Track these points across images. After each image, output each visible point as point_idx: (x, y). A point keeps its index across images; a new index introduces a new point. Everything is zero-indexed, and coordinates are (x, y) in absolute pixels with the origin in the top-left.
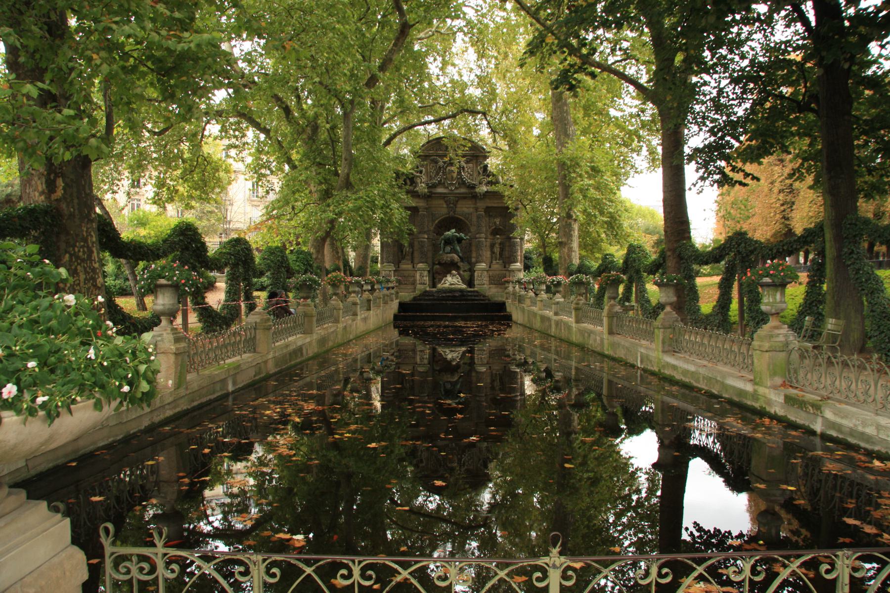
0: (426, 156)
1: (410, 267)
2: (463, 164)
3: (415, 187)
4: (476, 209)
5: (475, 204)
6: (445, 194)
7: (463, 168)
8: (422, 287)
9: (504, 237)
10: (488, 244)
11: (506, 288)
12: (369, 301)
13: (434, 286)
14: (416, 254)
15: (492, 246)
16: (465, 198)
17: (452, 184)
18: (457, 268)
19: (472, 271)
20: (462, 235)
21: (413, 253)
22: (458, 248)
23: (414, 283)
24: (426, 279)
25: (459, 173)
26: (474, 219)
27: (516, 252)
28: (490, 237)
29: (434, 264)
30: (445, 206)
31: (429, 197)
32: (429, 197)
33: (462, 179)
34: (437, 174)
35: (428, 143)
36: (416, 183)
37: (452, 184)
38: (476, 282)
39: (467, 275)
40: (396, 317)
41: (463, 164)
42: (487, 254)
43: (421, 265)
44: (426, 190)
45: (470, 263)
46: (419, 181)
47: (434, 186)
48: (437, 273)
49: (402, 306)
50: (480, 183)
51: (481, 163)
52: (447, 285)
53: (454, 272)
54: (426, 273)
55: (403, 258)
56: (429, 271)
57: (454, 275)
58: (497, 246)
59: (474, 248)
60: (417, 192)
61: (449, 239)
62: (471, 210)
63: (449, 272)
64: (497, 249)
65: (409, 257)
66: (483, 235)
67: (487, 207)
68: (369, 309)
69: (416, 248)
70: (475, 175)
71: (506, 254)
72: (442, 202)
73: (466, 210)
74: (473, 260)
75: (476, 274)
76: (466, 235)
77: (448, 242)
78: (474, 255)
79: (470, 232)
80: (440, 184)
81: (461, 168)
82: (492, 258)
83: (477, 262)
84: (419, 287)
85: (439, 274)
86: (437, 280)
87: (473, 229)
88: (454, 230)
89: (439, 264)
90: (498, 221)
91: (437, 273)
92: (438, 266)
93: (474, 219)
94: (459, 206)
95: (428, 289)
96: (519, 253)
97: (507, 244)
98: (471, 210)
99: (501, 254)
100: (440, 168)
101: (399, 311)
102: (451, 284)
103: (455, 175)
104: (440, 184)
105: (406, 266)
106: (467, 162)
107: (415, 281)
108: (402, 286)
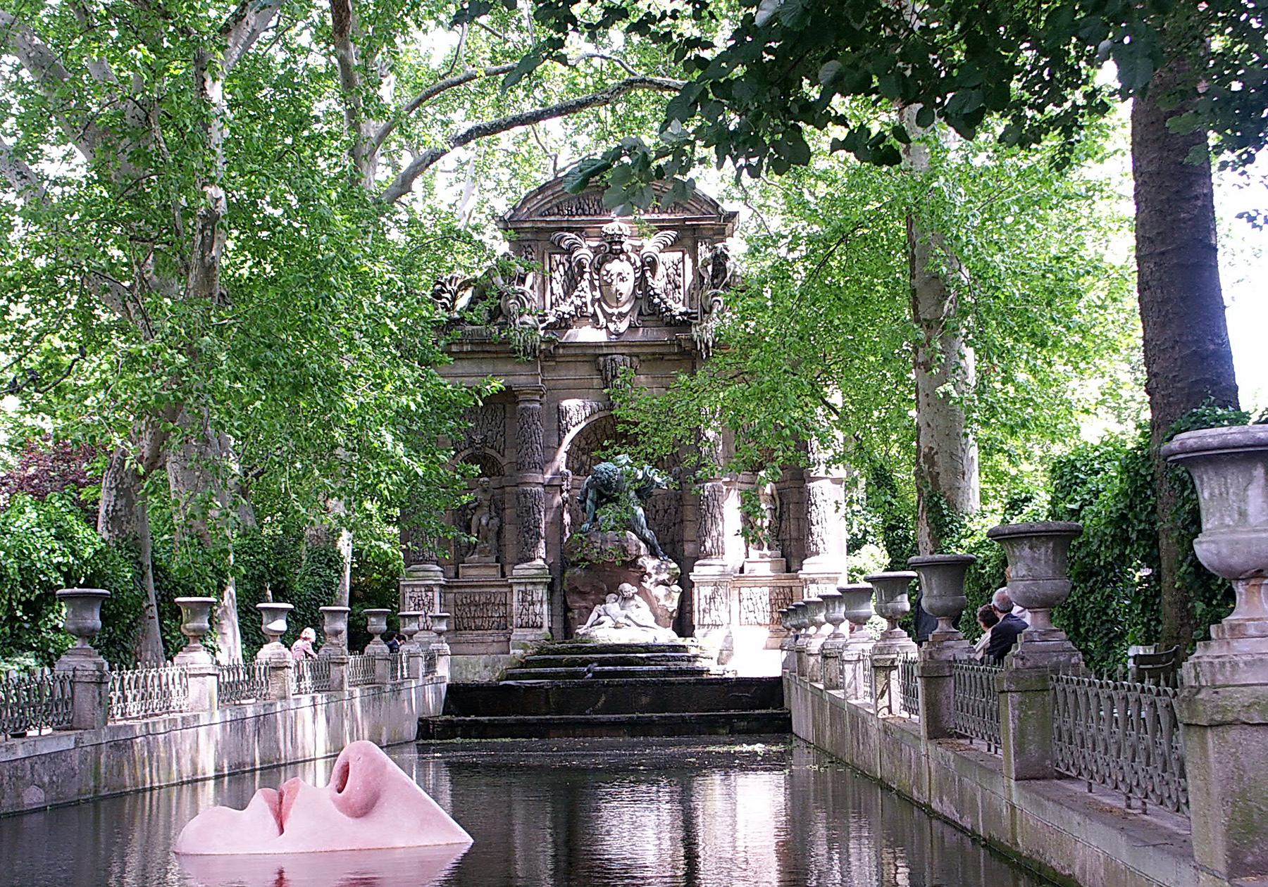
1: (494, 572)
3: (503, 326)
6: (597, 345)
8: (530, 635)
13: (568, 632)
21: (499, 533)
23: (504, 625)
25: (641, 282)
30: (597, 382)
31: (549, 356)
32: (549, 356)
40: (426, 728)
48: (575, 590)
53: (627, 588)
54: (541, 593)
56: (550, 587)
59: (689, 513)
60: (507, 341)
63: (614, 588)
71: (791, 527)
74: (689, 548)
77: (605, 492)
78: (689, 533)
84: (517, 634)
85: (583, 595)
91: (575, 590)
103: (626, 288)
105: (478, 571)
107: (507, 617)
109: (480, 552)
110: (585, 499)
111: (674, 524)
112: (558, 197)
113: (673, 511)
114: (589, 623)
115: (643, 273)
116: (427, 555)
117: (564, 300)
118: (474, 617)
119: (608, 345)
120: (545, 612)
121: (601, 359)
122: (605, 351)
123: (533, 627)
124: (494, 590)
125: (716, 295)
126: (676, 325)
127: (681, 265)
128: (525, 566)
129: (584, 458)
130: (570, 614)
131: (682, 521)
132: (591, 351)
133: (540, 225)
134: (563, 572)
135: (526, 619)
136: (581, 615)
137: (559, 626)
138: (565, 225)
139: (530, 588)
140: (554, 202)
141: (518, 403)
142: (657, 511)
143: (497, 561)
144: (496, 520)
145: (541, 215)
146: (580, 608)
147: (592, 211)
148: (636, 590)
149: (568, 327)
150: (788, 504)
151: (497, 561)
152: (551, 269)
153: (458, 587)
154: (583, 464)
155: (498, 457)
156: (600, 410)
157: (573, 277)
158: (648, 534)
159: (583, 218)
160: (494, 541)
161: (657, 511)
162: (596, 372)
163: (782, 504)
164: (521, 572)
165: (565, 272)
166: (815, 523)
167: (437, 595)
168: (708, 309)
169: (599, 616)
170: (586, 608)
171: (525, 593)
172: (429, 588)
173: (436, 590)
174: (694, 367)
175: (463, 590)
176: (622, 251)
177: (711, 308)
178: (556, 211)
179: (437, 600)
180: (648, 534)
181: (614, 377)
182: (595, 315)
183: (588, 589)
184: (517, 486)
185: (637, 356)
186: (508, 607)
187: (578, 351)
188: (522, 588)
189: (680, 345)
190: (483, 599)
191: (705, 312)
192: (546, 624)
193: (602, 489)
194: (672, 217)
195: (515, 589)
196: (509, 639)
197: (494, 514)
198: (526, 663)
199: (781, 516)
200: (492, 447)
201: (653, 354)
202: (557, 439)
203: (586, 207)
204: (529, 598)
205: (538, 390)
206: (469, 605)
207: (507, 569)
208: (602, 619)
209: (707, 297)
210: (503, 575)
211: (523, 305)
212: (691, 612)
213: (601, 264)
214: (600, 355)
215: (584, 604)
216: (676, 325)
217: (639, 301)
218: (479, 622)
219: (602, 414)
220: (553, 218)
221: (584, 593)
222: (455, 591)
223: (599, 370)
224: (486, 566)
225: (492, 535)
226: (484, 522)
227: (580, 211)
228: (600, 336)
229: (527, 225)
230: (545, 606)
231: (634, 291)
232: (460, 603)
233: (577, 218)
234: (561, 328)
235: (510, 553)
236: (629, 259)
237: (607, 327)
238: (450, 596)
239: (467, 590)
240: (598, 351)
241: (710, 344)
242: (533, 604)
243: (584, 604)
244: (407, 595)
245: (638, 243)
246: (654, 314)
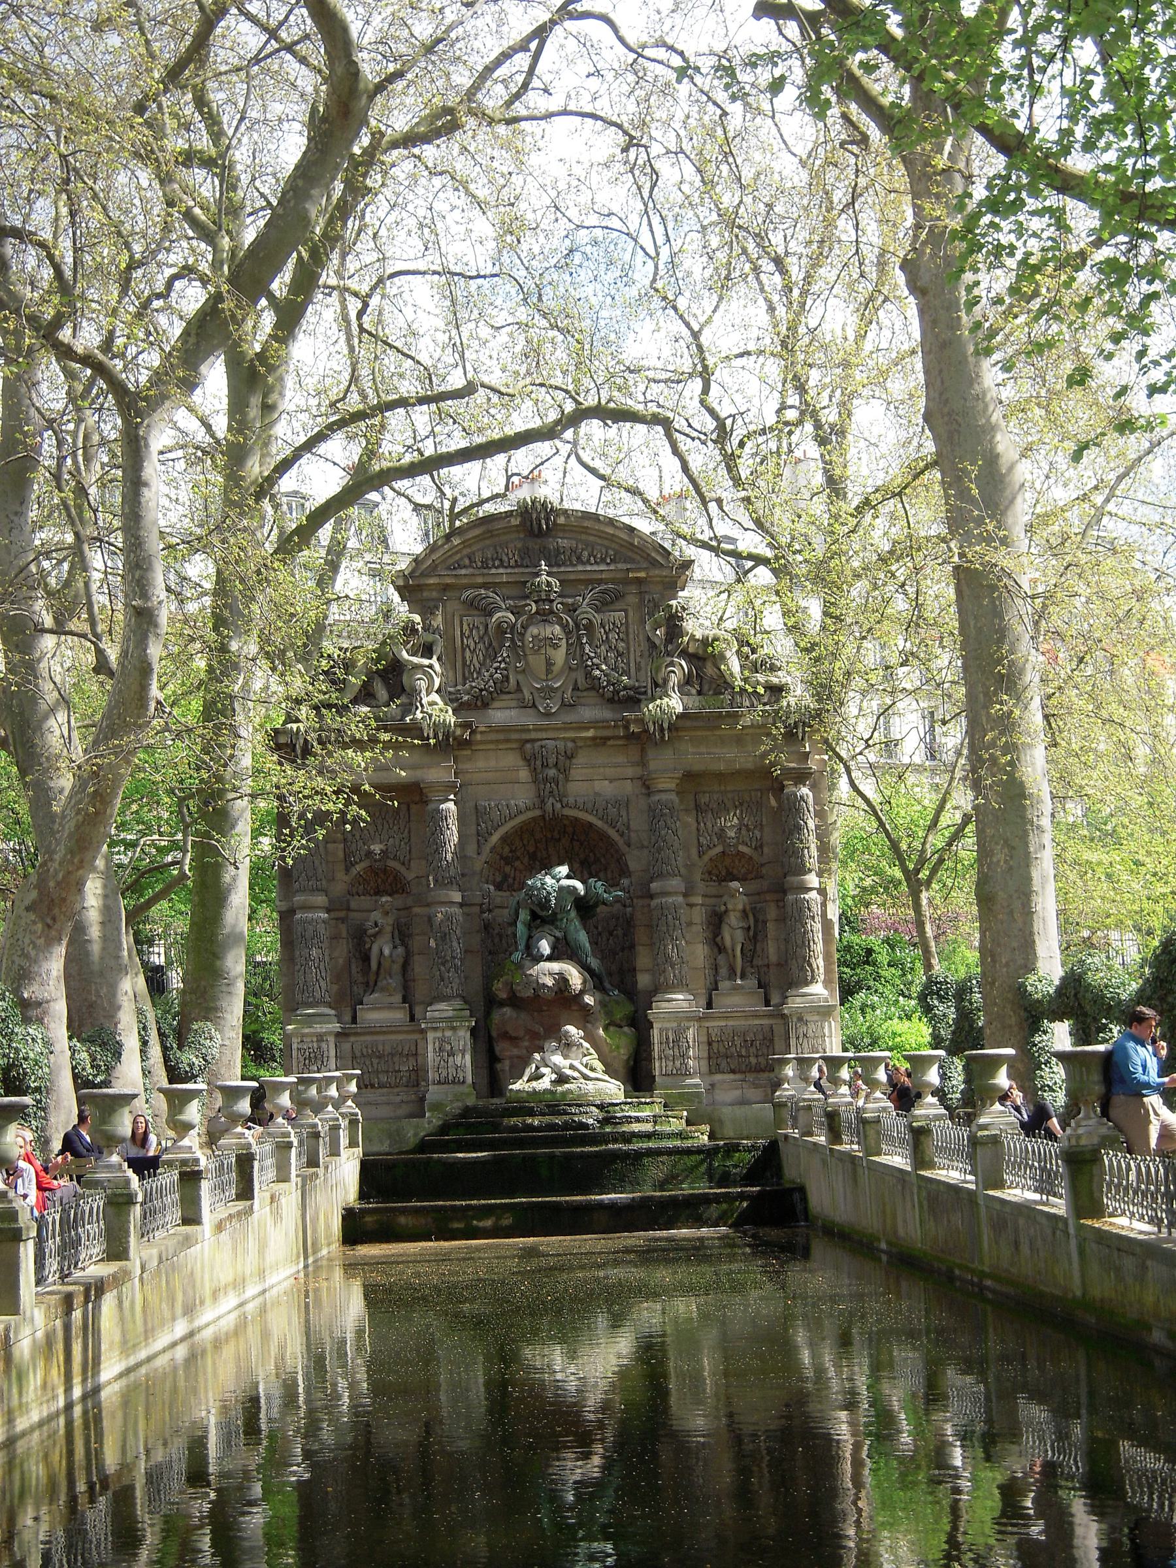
0: (446, 588)
1: (399, 1016)
2: (586, 611)
3: (409, 708)
4: (646, 785)
5: (643, 763)
6: (525, 729)
7: (590, 627)
9: (754, 886)
10: (698, 916)
11: (777, 1085)
12: (245, 1162)
14: (419, 967)
15: (716, 921)
16: (599, 742)
17: (548, 692)
18: (584, 1017)
19: (639, 1025)
20: (599, 887)
21: (406, 965)
22: (583, 938)
24: (466, 1060)
25: (575, 649)
26: (638, 822)
27: (804, 942)
28: (701, 887)
29: (491, 1002)
30: (524, 774)
32: (463, 744)
33: (588, 675)
34: (492, 653)
35: (448, 537)
36: (414, 693)
37: (548, 692)
38: (657, 1067)
39: (622, 1045)
40: (349, 1216)
41: (586, 611)
42: (698, 953)
43: (443, 1009)
44: (450, 718)
45: (630, 992)
46: (423, 684)
47: (480, 702)
48: (505, 1036)
49: (369, 1171)
50: (659, 687)
51: (656, 606)
52: (544, 1084)
53: (571, 1029)
54: (463, 1038)
55: (370, 986)
56: (474, 1032)
57: (567, 1046)
58: (733, 919)
59: (641, 935)
61: (544, 904)
62: (628, 787)
63: (553, 1031)
64: (733, 935)
65: (394, 982)
66: (675, 883)
67: (690, 777)
68: (246, 1192)
69: (416, 943)
70: (637, 648)
71: (772, 950)
72: (511, 759)
73: (606, 789)
74: (643, 980)
75: (655, 1033)
76: (612, 884)
78: (643, 959)
79: (624, 871)
80: (501, 689)
81: (578, 632)
82: (716, 968)
83: (658, 989)
84: (434, 1093)
85: (514, 1040)
86: (506, 1065)
87: (635, 861)
88: (563, 870)
89: (514, 1001)
90: (730, 822)
91: (505, 1036)
92: (507, 1011)
93: (638, 822)
94: (575, 773)
95: (471, 1101)
96: (819, 947)
97: (772, 913)
98: (628, 787)
99: (751, 953)
100: (500, 630)
101: (363, 1195)
102: (562, 1079)
103: (559, 656)
104: (501, 689)
106: (604, 604)
108: (370, 1095)
109: (383, 990)
110: (514, 923)
111: (623, 949)
112: (470, 546)
113: (620, 932)
114: (525, 1078)
115: (579, 638)
116: (317, 995)
117: (479, 673)
118: (378, 1072)
119: (538, 729)
120: (469, 1064)
121: (528, 746)
122: (533, 735)
123: (453, 1082)
124: (400, 1037)
125: (672, 664)
126: (620, 701)
127: (623, 629)
128: (442, 1006)
129: (507, 869)
130: (499, 1066)
131: (632, 947)
132: (514, 736)
133: (448, 581)
134: (488, 1014)
135: (444, 1074)
136: (511, 1067)
137: (484, 1082)
138: (480, 580)
139: (448, 1033)
140: (465, 552)
141: (426, 803)
142: (600, 934)
143: (404, 1002)
144: (400, 950)
145: (449, 568)
146: (511, 1058)
147: (512, 563)
148: (581, 1033)
149: (486, 705)
150: (765, 922)
151: (404, 1002)
152: (462, 634)
153: (356, 1034)
154: (506, 877)
155: (402, 870)
156: (528, 809)
157: (490, 644)
158: (594, 963)
159: (501, 571)
160: (400, 977)
161: (600, 934)
162: (521, 763)
163: (756, 921)
164: (436, 1014)
165: (481, 638)
166: (799, 942)
167: (332, 1046)
168: (660, 681)
169: (537, 1068)
170: (519, 1057)
171: (442, 1040)
172: (320, 1038)
173: (332, 1039)
174: (643, 751)
175: (362, 1038)
176: (551, 612)
177: (666, 681)
178: (467, 561)
179: (332, 1053)
180: (594, 963)
181: (545, 766)
182: (519, 689)
183: (521, 1033)
184: (428, 905)
185: (573, 740)
186: (420, 1059)
187: (501, 736)
188: (439, 1034)
189: (626, 727)
190: (388, 1049)
191: (657, 685)
192: (469, 1080)
193: (538, 910)
194: (612, 567)
195: (431, 1036)
196: (422, 1099)
197: (398, 942)
198: (444, 1129)
199: (755, 934)
200: (395, 859)
201: (594, 738)
202: (475, 846)
203: (505, 558)
204: (448, 1047)
205: (451, 787)
206: (370, 1056)
207: (418, 1011)
208: (543, 1070)
209: (658, 669)
210: (412, 1019)
211: (431, 679)
212: (650, 1059)
213: (525, 628)
214: (527, 741)
215: (516, 1052)
216: (620, 701)
217: (574, 675)
218: (384, 1078)
219: (530, 814)
220: (463, 572)
221: (516, 1038)
222: (352, 1039)
223: (525, 759)
224: (390, 1007)
225: (397, 968)
226: (387, 952)
227: (497, 563)
228: (528, 719)
229: (431, 581)
230: (468, 1057)
231: (567, 660)
232: (358, 1054)
233: (493, 571)
234: (476, 707)
235: (420, 991)
236: (560, 621)
237: (534, 706)
238: (346, 1046)
239: (368, 1038)
240: (525, 736)
241: (666, 725)
242: (451, 1054)
243: (516, 1052)
244: (295, 1046)
245: (570, 601)
246: (593, 688)
